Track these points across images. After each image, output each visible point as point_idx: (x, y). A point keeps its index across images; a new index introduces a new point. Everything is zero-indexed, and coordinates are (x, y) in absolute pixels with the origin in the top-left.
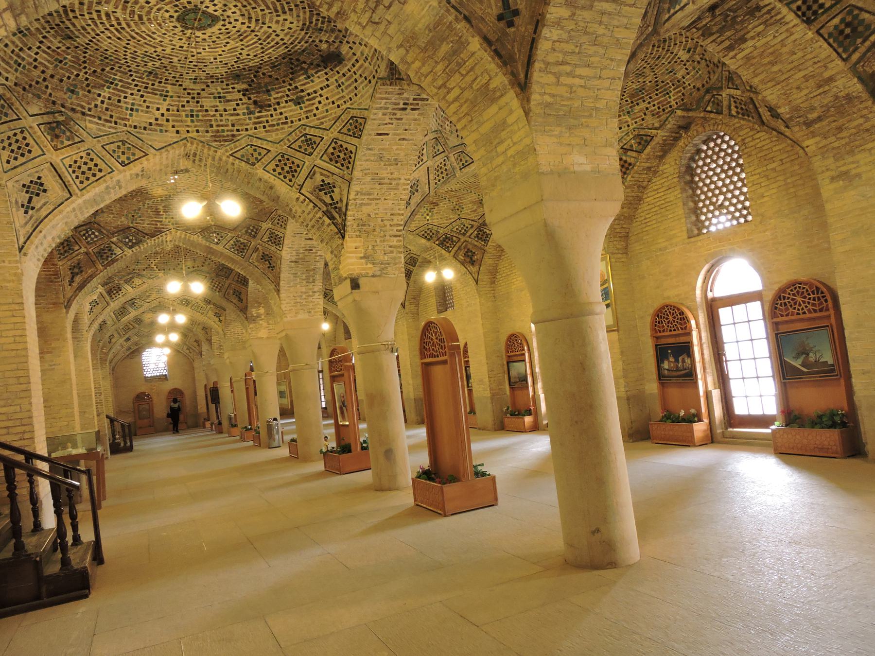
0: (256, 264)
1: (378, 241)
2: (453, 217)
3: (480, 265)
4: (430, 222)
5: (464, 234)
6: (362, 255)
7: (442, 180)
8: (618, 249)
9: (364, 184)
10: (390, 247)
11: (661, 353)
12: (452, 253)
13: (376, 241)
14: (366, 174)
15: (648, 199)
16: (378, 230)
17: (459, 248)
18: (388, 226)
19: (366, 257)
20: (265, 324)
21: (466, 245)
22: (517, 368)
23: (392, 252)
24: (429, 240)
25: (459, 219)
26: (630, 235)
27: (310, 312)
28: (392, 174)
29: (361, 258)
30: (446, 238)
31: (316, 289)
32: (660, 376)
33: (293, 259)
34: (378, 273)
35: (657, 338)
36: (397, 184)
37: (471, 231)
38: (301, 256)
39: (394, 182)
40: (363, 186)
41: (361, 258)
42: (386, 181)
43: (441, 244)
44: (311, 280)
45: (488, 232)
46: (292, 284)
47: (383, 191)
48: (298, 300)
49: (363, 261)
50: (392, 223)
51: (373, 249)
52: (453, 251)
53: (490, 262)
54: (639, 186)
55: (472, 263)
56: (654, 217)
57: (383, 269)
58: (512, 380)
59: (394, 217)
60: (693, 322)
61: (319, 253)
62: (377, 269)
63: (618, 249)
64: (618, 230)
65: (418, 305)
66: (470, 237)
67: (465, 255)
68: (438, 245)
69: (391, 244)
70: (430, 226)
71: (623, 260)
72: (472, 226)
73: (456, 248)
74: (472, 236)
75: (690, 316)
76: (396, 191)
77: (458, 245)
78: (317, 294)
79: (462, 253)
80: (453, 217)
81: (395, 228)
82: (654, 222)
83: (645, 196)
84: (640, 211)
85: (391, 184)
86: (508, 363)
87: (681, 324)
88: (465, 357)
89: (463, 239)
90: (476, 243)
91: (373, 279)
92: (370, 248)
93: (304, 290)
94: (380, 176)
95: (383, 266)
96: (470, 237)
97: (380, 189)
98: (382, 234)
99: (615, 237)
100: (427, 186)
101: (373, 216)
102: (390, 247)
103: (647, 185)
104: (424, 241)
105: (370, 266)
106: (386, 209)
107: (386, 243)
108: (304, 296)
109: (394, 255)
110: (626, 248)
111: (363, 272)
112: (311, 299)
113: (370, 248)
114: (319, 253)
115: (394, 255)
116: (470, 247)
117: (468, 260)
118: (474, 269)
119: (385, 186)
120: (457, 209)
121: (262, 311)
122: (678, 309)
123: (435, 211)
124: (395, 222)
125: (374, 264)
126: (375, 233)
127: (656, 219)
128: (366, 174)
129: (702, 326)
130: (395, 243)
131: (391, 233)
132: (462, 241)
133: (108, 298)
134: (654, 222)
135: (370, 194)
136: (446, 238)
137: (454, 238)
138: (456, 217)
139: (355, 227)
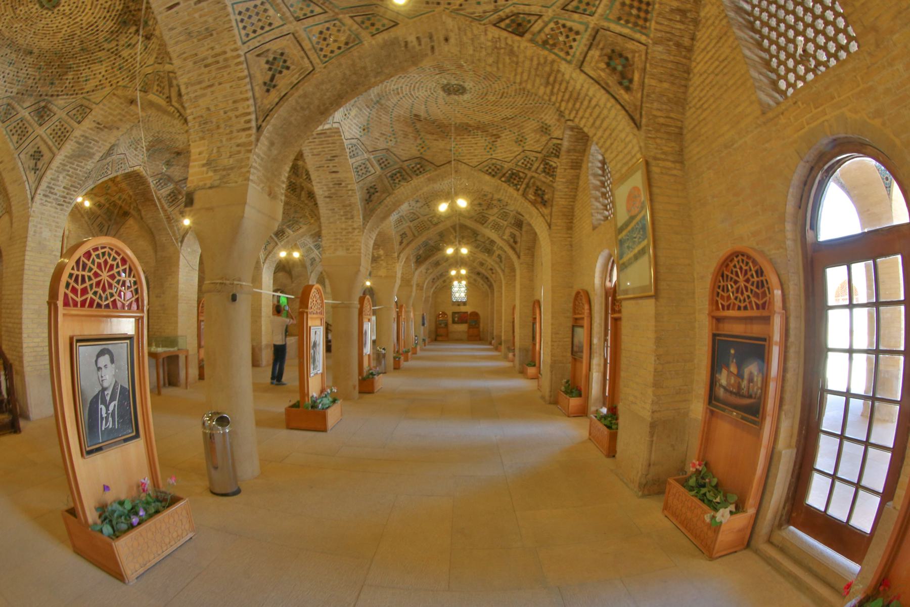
0: (306, 202)
1: (224, 140)
2: (517, 149)
3: (552, 206)
4: (494, 156)
5: (530, 169)
6: (205, 162)
7: (337, 52)
8: (664, 153)
9: (189, 72)
10: (238, 146)
11: (721, 350)
12: (521, 192)
13: (221, 141)
14: (185, 59)
15: (698, 68)
16: (222, 126)
17: (528, 185)
18: (234, 119)
19: (208, 164)
20: (384, 264)
21: (534, 183)
22: (581, 334)
23: (239, 152)
24: (493, 176)
25: (523, 151)
26: (685, 131)
27: (348, 249)
28: (212, 48)
29: (204, 165)
30: (513, 174)
31: (355, 226)
32: (712, 397)
33: (326, 194)
34: (217, 183)
35: (719, 320)
36: (226, 60)
37: (536, 165)
38: (333, 191)
39: (221, 58)
40: (190, 75)
41: (204, 165)
42: (210, 60)
43: (508, 181)
44: (349, 216)
45: (554, 165)
46: (331, 220)
47: (214, 74)
48: (339, 237)
49: (205, 169)
50: (237, 113)
51: (218, 152)
52: (521, 189)
53: (563, 202)
54: (678, 45)
55: (544, 203)
56: (711, 93)
57: (224, 176)
58: (575, 349)
59: (237, 105)
60: (778, 293)
61: (349, 187)
62: (217, 177)
63: (664, 153)
64: (661, 120)
65: (533, 256)
66: (536, 171)
67: (536, 194)
68: (505, 182)
69: (239, 141)
70: (494, 161)
71: (675, 172)
72: (537, 158)
73: (524, 186)
74: (539, 171)
75: (773, 280)
76: (228, 70)
77: (526, 181)
78: (357, 231)
79: (531, 191)
80: (517, 149)
81: (243, 120)
82: (711, 100)
83: (694, 64)
84: (691, 89)
85: (218, 62)
86: (573, 326)
87: (756, 295)
88: (614, 311)
89: (530, 174)
90: (544, 179)
91: (210, 192)
92: (215, 151)
93: (343, 226)
94: (201, 56)
95: (224, 173)
96: (536, 171)
97: (209, 72)
98: (228, 131)
99: (658, 131)
100: (306, 60)
101: (213, 109)
102: (238, 146)
103: (692, 46)
104: (487, 178)
105: (211, 174)
106: (225, 97)
107: (233, 141)
108: (344, 233)
109: (241, 156)
110: (681, 152)
111: (201, 184)
112: (350, 236)
113: (215, 151)
114: (349, 187)
115: (241, 156)
116: (539, 184)
117: (539, 200)
118: (546, 211)
119: (213, 67)
120: (520, 140)
121: (381, 252)
122: (755, 262)
123: (498, 143)
124: (241, 111)
125: (215, 171)
126: (221, 130)
127: (713, 95)
128: (185, 59)
129: (792, 305)
130: (244, 140)
131: (240, 127)
132: (529, 176)
133: (276, 239)
134: (711, 100)
135: (200, 83)
136: (513, 174)
137: (521, 174)
138: (521, 149)
139: (196, 127)
